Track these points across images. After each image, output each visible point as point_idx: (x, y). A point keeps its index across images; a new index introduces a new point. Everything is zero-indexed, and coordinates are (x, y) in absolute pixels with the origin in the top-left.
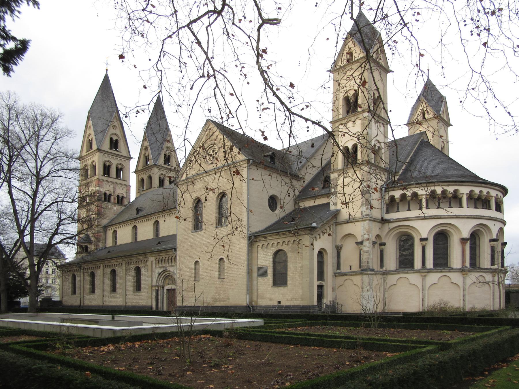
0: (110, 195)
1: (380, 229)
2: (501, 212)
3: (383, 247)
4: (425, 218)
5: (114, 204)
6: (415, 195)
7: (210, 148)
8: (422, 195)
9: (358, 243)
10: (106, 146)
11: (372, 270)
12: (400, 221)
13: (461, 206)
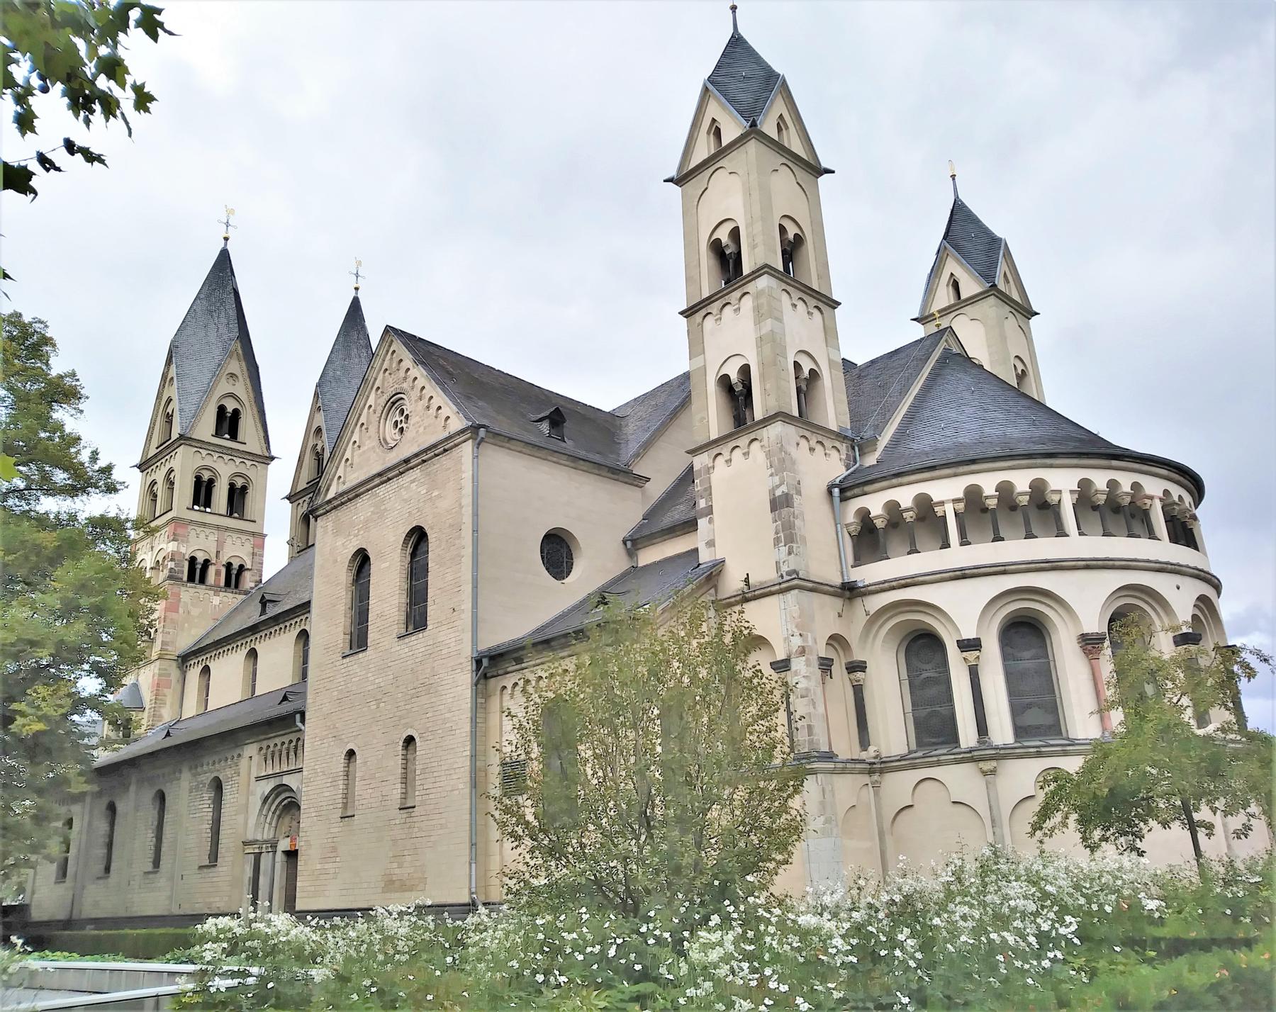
0: (207, 563)
1: (840, 616)
2: (1196, 548)
3: (859, 675)
4: (962, 575)
5: (216, 588)
6: (925, 506)
7: (394, 403)
8: (942, 503)
9: (782, 666)
10: (206, 428)
11: (829, 756)
12: (893, 588)
13: (1062, 533)
